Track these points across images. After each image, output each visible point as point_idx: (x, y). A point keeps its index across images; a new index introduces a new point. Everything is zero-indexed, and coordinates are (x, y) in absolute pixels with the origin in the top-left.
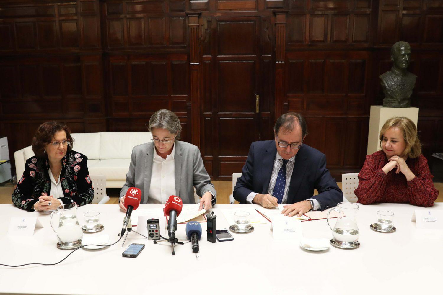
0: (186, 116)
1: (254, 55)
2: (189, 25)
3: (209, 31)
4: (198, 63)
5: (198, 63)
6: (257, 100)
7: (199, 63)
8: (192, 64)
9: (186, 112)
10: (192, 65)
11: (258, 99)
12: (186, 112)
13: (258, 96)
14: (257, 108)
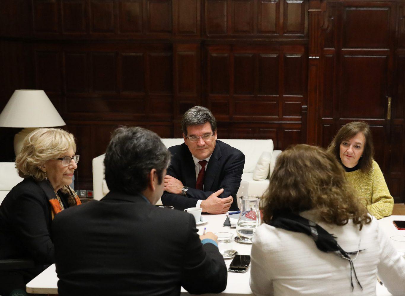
0: (299, 121)
1: (386, 48)
2: (309, 10)
3: (332, 18)
4: (318, 58)
5: (318, 58)
6: (389, 104)
7: (319, 57)
8: (310, 57)
9: (300, 117)
10: (311, 59)
11: (389, 102)
12: (300, 117)
13: (390, 99)
14: (389, 113)
